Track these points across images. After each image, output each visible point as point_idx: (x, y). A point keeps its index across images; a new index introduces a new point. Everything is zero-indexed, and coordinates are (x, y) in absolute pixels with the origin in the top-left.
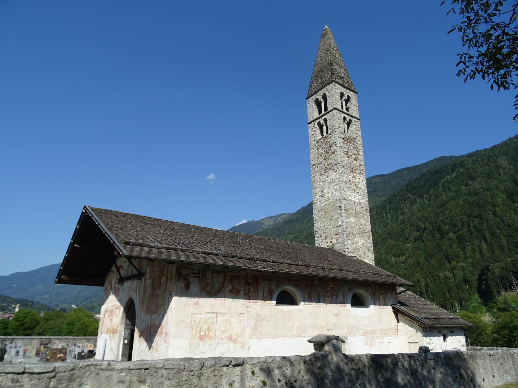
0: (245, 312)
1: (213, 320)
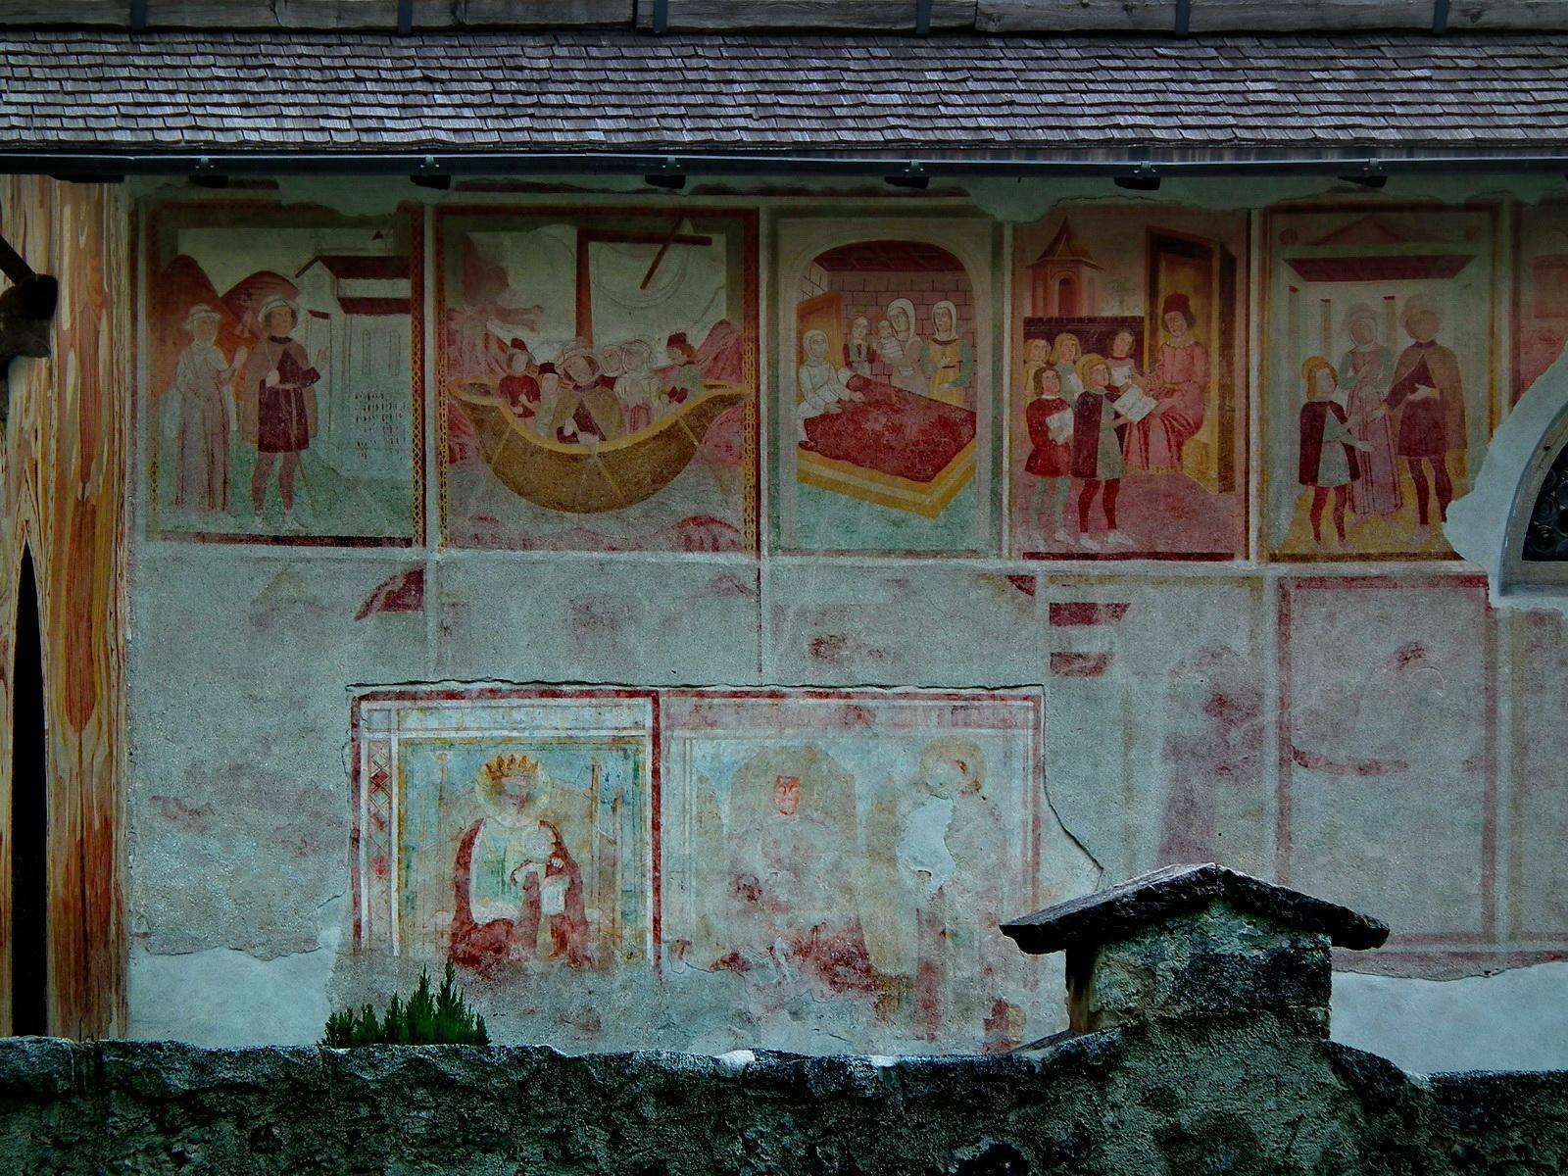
0: (1034, 668)
1: (614, 766)
